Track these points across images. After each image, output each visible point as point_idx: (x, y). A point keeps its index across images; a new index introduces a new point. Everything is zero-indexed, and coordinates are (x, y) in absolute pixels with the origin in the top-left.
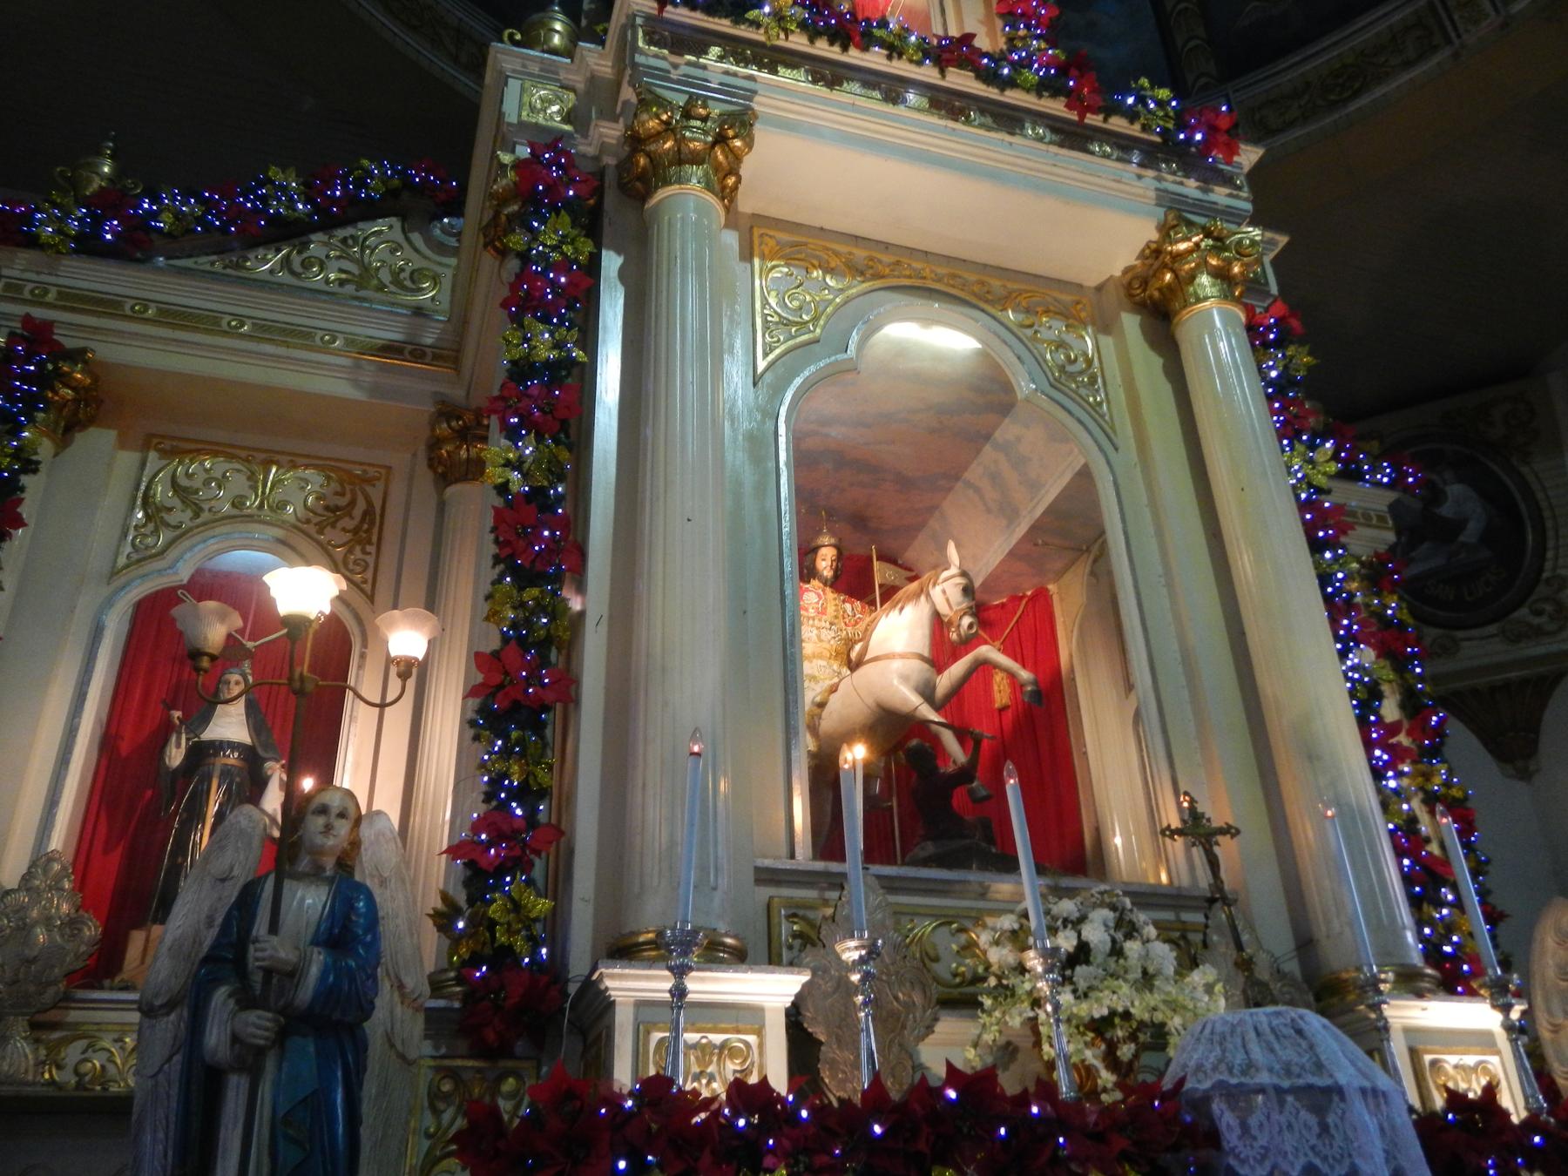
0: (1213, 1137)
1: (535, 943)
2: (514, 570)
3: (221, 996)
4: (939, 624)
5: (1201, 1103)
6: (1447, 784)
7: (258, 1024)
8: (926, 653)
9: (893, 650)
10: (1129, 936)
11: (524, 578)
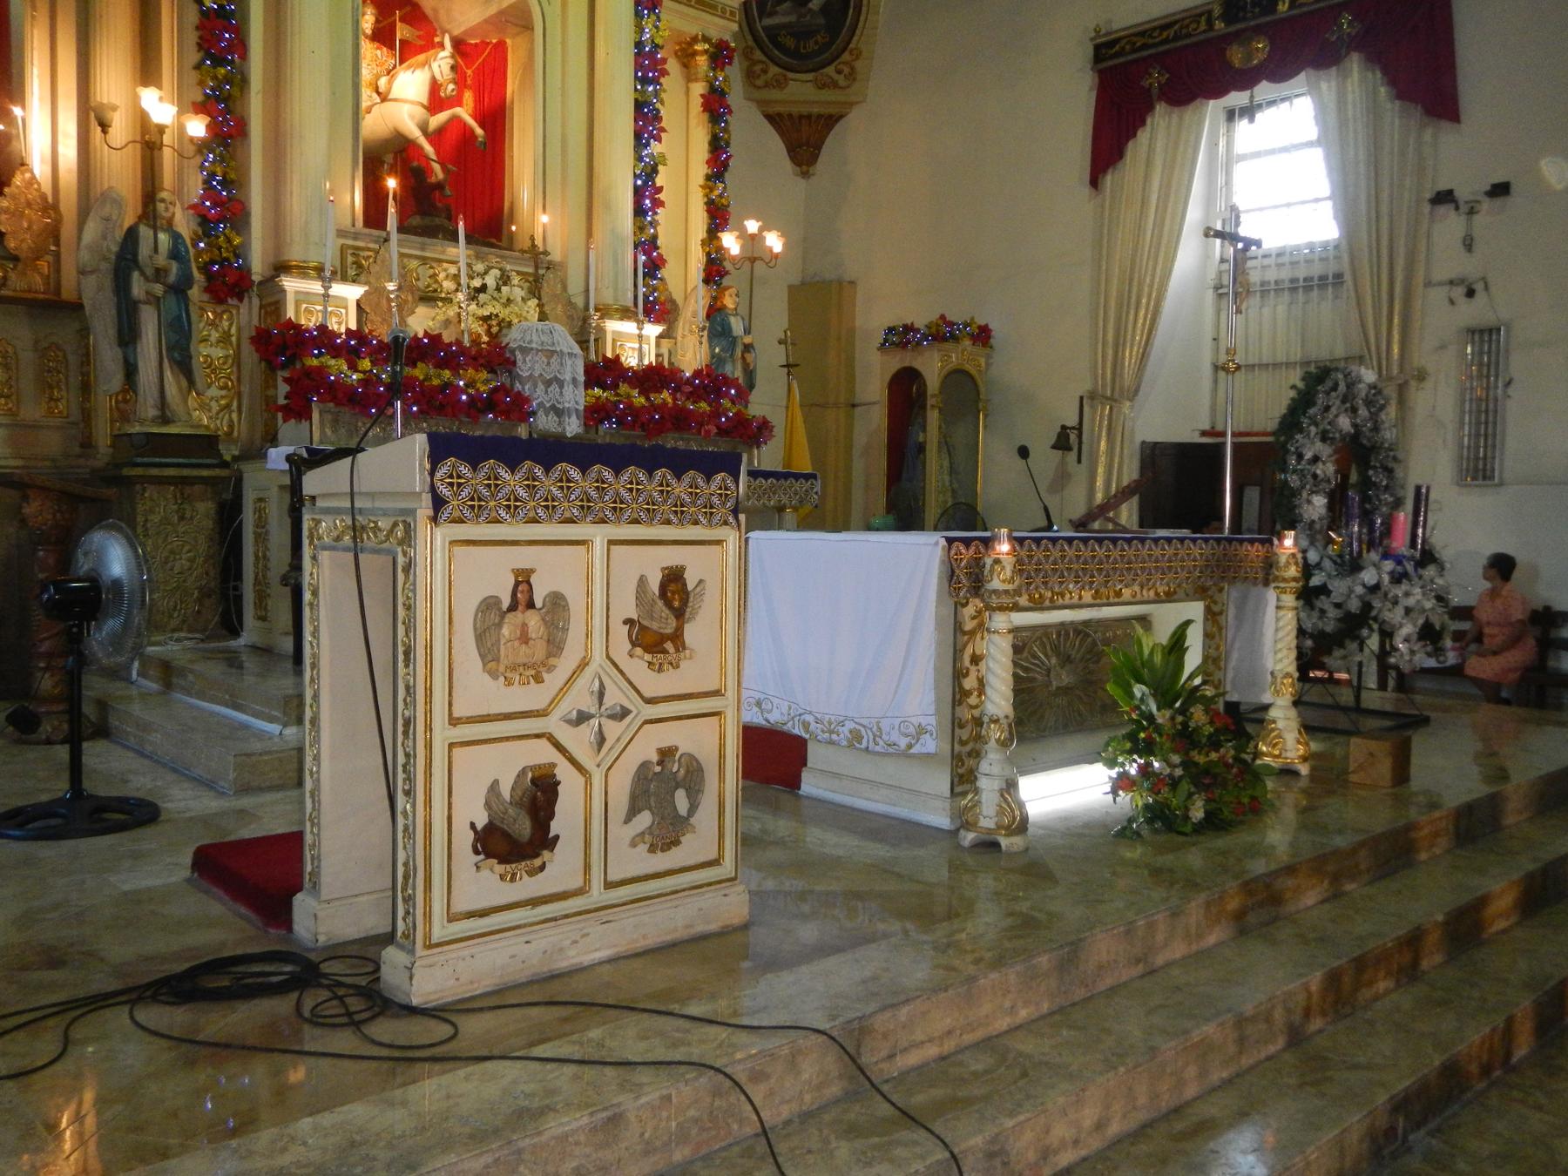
0: (514, 363)
1: (237, 256)
2: (208, 55)
3: (136, 275)
4: (435, 87)
5: (513, 351)
6: (721, 196)
7: (158, 289)
8: (425, 102)
9: (405, 96)
10: (505, 284)
11: (219, 61)
